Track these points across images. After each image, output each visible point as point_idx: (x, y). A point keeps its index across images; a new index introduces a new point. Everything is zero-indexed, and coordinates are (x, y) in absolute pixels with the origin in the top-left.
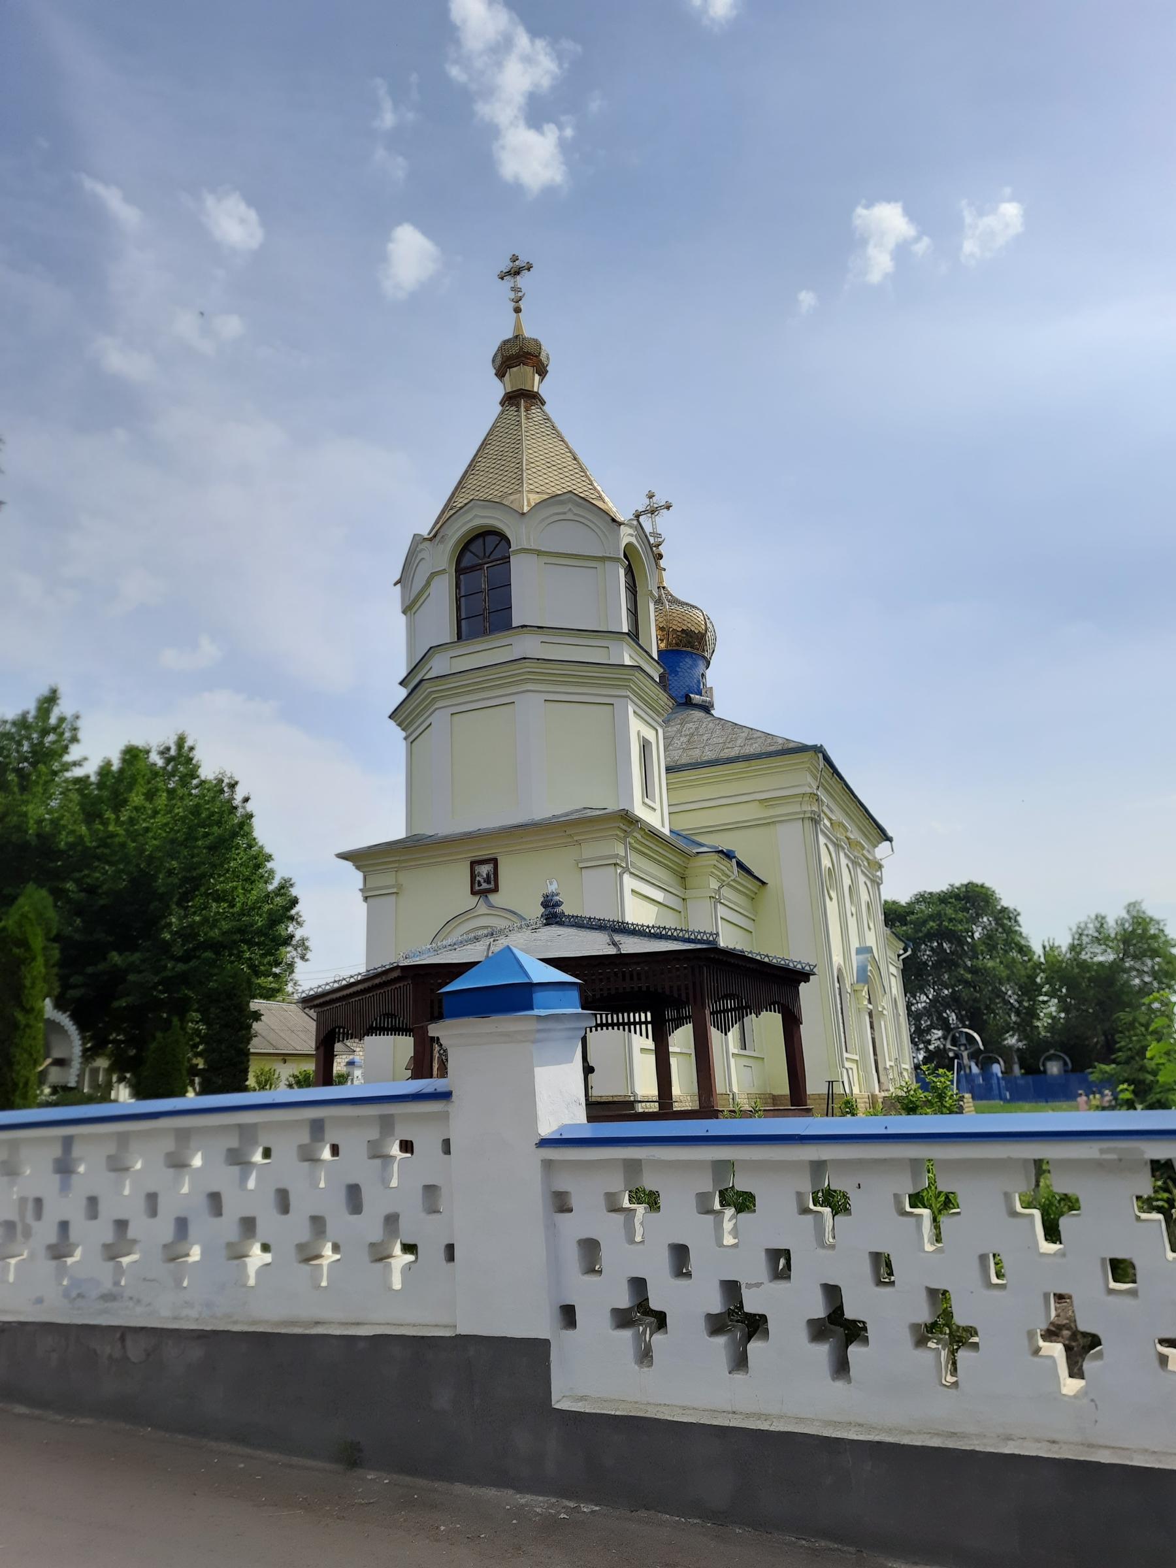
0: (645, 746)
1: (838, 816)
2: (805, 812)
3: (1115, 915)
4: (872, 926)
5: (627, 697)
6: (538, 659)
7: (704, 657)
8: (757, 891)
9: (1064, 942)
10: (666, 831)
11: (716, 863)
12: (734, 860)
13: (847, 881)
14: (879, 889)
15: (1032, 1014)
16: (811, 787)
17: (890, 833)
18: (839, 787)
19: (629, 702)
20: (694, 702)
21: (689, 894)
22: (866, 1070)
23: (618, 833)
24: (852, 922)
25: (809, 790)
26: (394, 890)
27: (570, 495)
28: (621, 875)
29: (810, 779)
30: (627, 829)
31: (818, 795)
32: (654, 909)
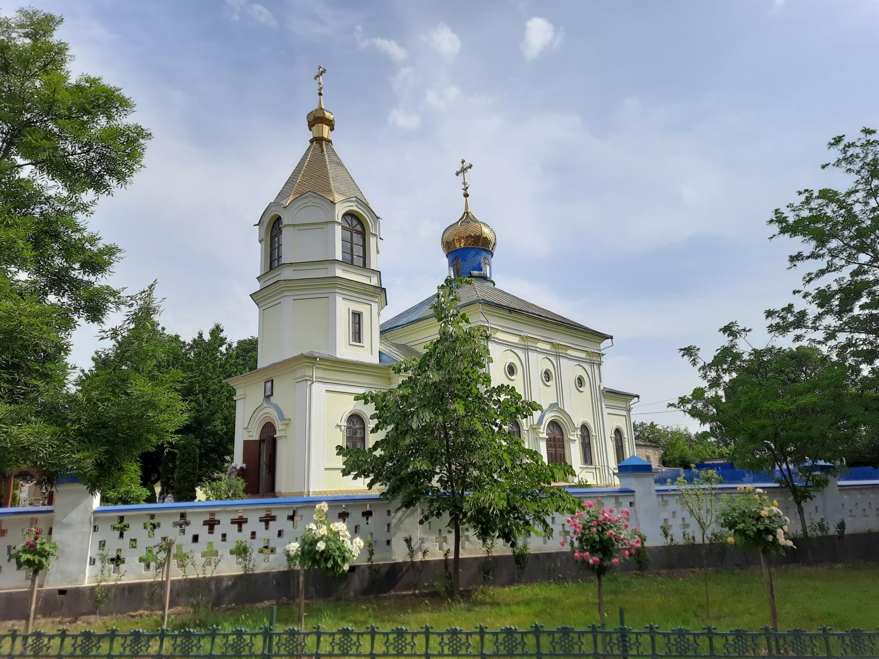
5: (336, 292)
26: (242, 397)
27: (309, 193)
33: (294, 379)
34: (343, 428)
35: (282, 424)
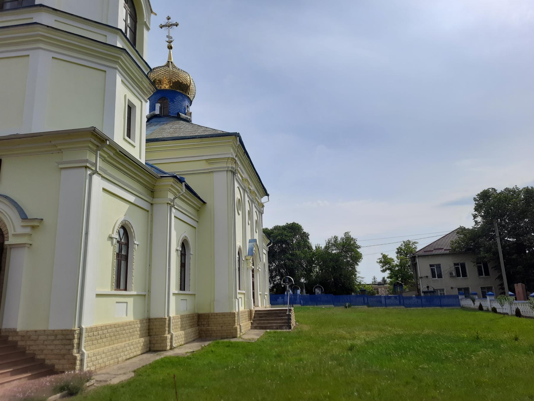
0: (130, 108)
1: (245, 176)
2: (228, 167)
3: (341, 236)
4: (257, 231)
5: (116, 69)
6: (48, 26)
7: (188, 97)
8: (200, 206)
9: (323, 245)
10: (143, 161)
11: (173, 184)
12: (184, 183)
13: (247, 208)
14: (262, 216)
15: (311, 271)
16: (232, 155)
17: (268, 193)
18: (247, 162)
19: (117, 71)
20: (181, 117)
21: (156, 200)
22: (249, 298)
23: (90, 145)
24: (248, 228)
25: (231, 156)
28: (91, 176)
29: (232, 151)
30: (98, 144)
31: (236, 160)
32: (127, 206)
33: (59, 163)
34: (115, 241)
35: (23, 226)
